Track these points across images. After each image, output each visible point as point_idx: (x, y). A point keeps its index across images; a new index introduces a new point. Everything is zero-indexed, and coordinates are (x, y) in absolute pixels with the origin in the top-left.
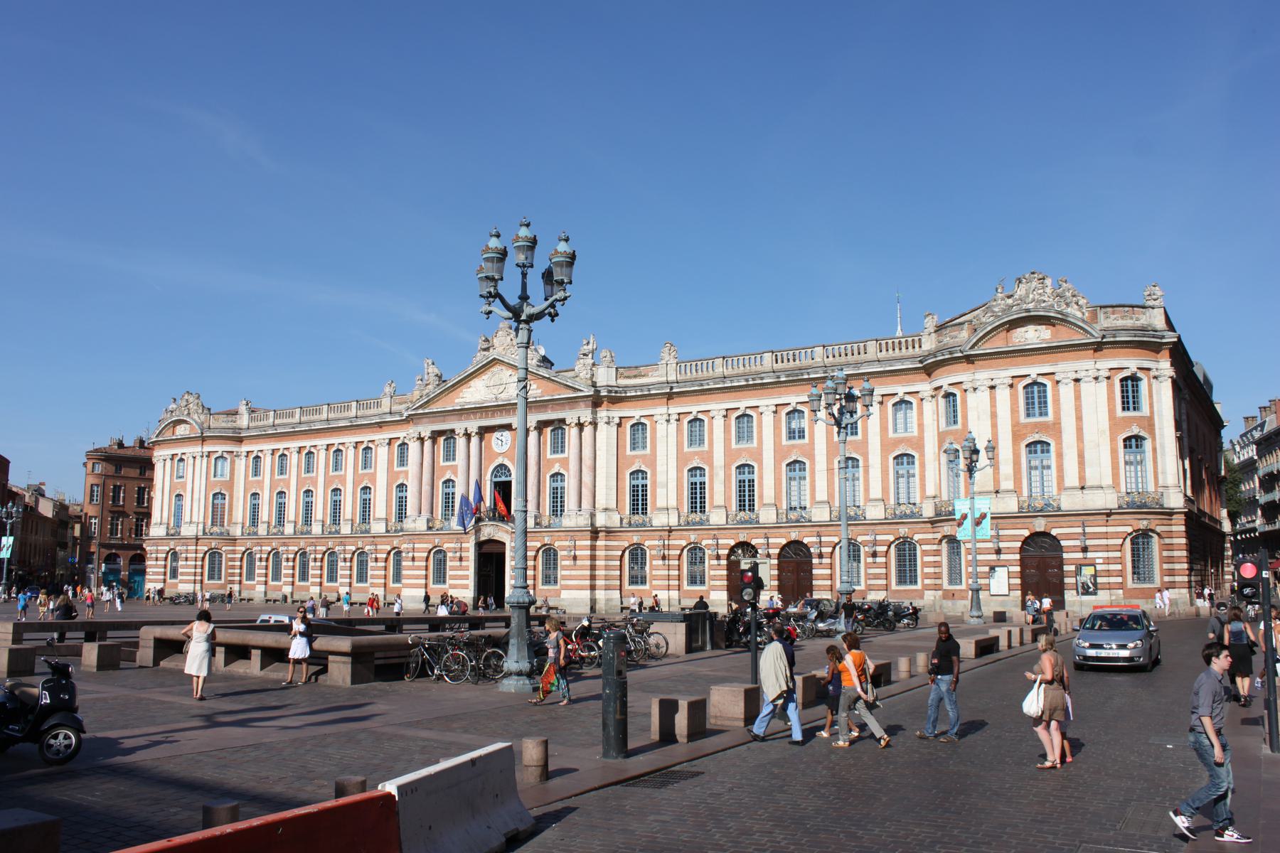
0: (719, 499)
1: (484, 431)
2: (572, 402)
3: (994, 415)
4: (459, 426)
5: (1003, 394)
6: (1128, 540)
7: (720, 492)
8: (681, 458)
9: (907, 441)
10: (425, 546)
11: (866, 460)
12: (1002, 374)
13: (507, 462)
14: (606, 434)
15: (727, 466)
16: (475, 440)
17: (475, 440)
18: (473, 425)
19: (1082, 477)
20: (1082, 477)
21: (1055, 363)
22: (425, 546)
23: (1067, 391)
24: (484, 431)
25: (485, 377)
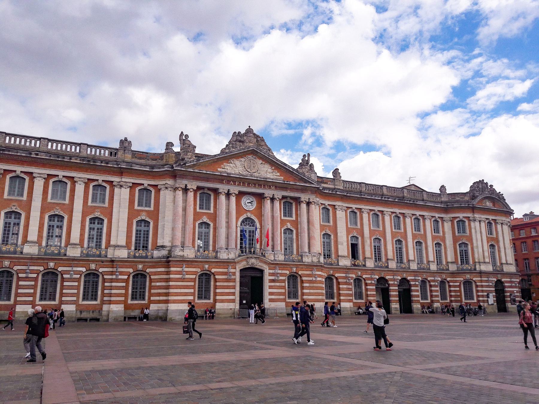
0: (368, 254)
1: (241, 194)
2: (304, 190)
3: (481, 232)
4: (223, 188)
5: (483, 224)
6: (462, 283)
7: (367, 249)
8: (348, 231)
9: (439, 237)
10: (194, 270)
11: (426, 243)
12: (484, 217)
13: (253, 217)
14: (316, 212)
15: (370, 237)
16: (233, 199)
17: (233, 199)
18: (235, 189)
19: (506, 261)
20: (506, 261)
21: (496, 216)
22: (194, 270)
23: (499, 227)
24: (241, 194)
25: (243, 160)
